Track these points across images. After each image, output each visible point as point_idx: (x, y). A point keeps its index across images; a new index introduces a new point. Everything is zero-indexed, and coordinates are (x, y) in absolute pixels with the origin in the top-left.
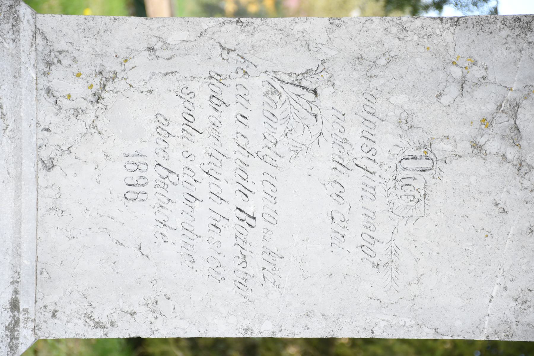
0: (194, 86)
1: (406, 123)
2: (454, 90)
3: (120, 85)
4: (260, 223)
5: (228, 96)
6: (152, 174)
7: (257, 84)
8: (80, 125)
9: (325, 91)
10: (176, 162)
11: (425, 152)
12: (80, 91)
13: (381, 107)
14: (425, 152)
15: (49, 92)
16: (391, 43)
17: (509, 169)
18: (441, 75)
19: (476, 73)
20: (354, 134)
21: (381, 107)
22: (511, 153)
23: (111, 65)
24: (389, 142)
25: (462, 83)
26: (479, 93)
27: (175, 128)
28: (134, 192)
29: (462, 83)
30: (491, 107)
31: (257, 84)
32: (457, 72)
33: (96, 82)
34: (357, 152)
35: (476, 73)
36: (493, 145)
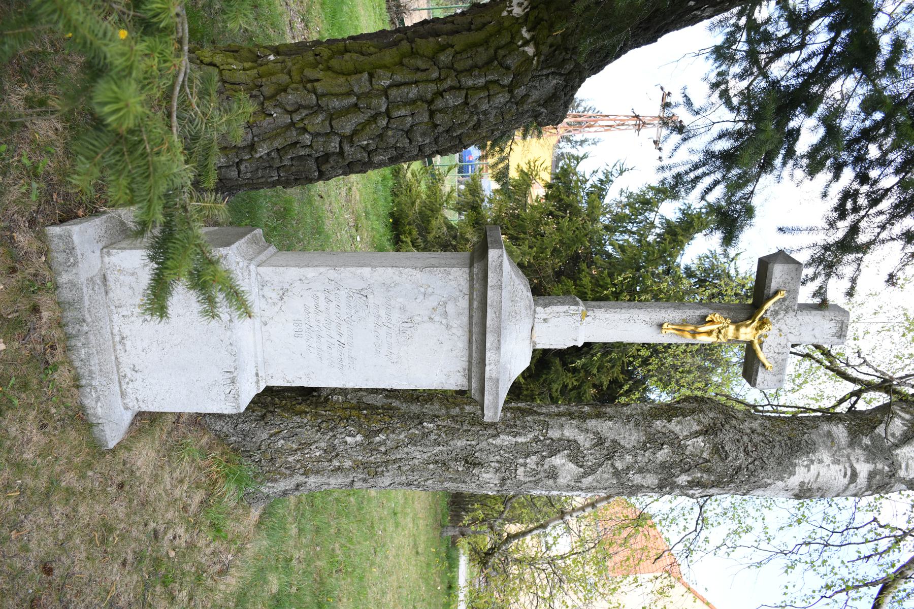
0: (318, 294)
1: (403, 309)
2: (421, 297)
3: (290, 293)
4: (347, 346)
5: (332, 298)
6: (304, 327)
7: (343, 293)
8: (276, 309)
9: (370, 296)
10: (313, 323)
11: (410, 321)
12: (275, 296)
13: (393, 302)
14: (410, 321)
15: (263, 296)
16: (396, 278)
17: (443, 327)
18: (416, 291)
19: (430, 290)
20: (382, 313)
21: (393, 302)
22: (444, 321)
23: (286, 286)
24: (396, 316)
25: (425, 294)
26: (431, 298)
27: (312, 310)
28: (298, 334)
29: (425, 294)
30: (436, 303)
31: (343, 293)
32: (422, 290)
33: (281, 292)
34: (384, 320)
35: (430, 290)
36: (437, 318)
